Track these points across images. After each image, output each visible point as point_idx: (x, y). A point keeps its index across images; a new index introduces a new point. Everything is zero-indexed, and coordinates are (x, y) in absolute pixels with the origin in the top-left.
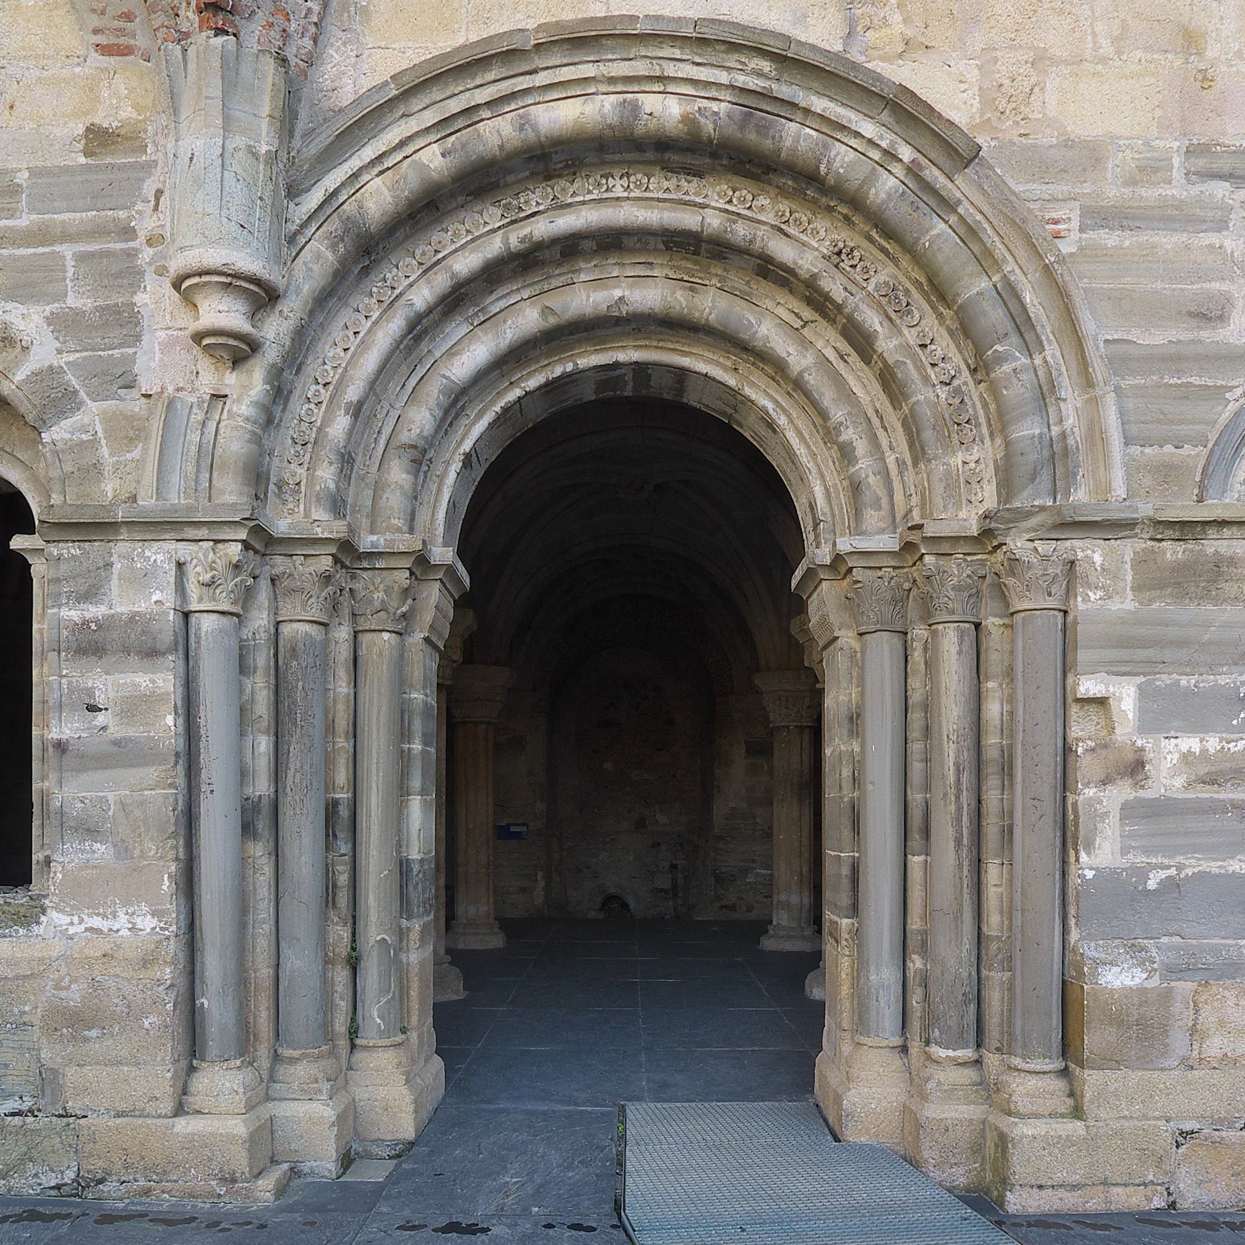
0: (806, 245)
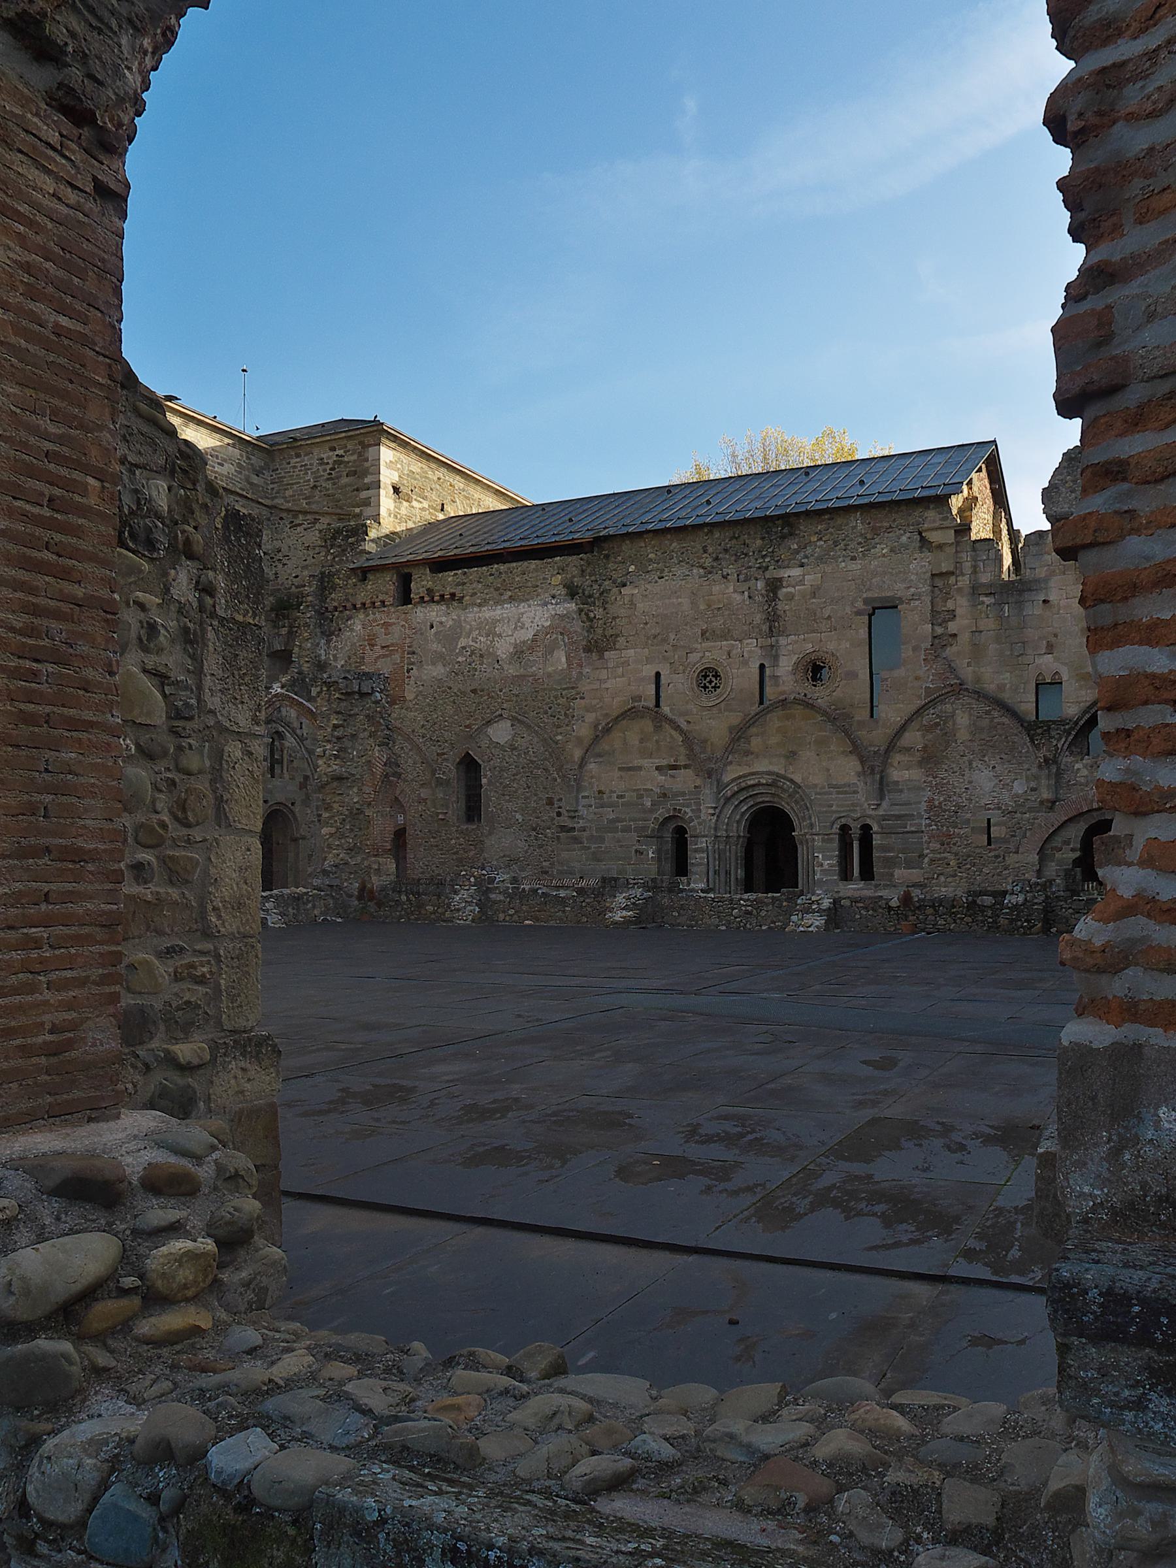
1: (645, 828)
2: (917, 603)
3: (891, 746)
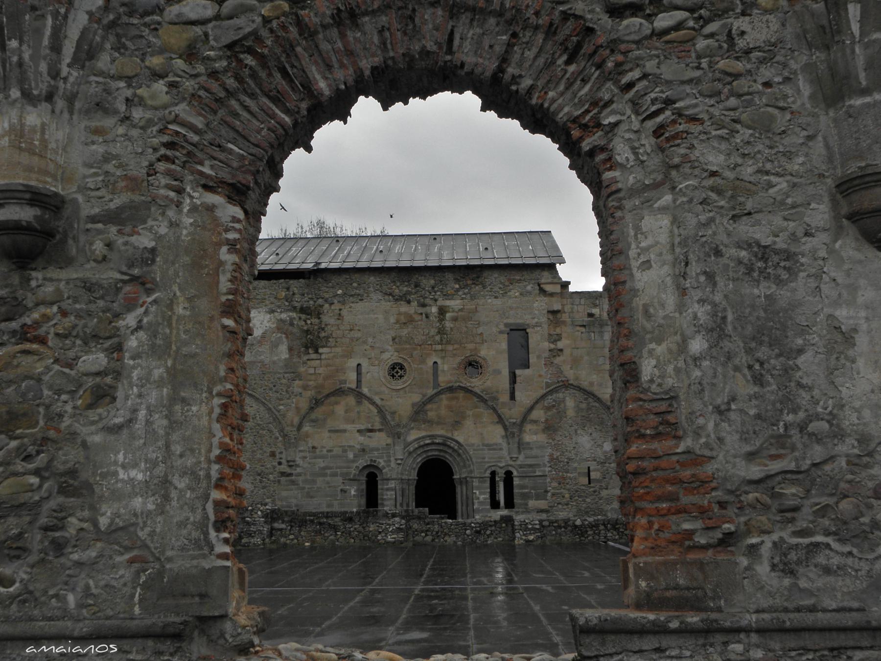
0: (450, 451)
1: (348, 474)
2: (539, 328)
3: (525, 419)
